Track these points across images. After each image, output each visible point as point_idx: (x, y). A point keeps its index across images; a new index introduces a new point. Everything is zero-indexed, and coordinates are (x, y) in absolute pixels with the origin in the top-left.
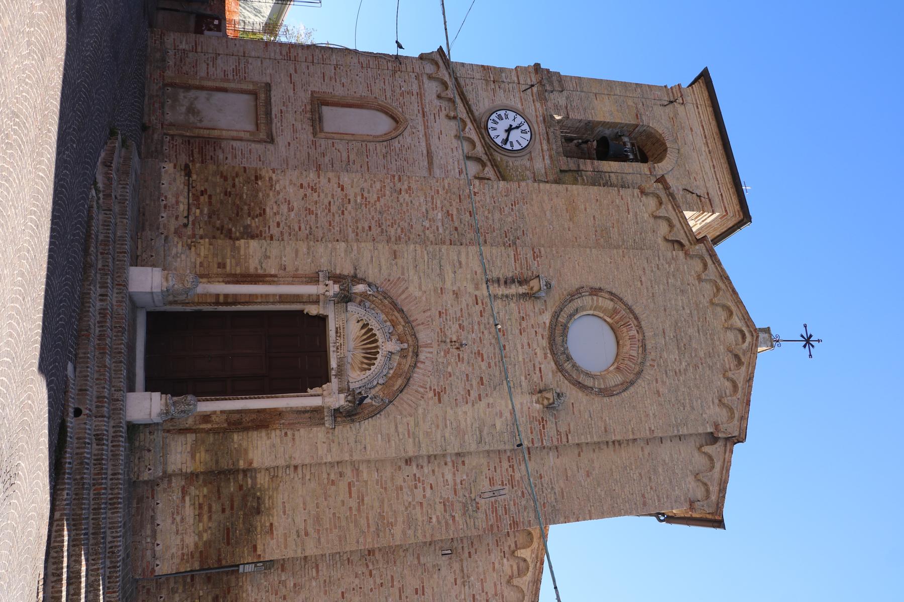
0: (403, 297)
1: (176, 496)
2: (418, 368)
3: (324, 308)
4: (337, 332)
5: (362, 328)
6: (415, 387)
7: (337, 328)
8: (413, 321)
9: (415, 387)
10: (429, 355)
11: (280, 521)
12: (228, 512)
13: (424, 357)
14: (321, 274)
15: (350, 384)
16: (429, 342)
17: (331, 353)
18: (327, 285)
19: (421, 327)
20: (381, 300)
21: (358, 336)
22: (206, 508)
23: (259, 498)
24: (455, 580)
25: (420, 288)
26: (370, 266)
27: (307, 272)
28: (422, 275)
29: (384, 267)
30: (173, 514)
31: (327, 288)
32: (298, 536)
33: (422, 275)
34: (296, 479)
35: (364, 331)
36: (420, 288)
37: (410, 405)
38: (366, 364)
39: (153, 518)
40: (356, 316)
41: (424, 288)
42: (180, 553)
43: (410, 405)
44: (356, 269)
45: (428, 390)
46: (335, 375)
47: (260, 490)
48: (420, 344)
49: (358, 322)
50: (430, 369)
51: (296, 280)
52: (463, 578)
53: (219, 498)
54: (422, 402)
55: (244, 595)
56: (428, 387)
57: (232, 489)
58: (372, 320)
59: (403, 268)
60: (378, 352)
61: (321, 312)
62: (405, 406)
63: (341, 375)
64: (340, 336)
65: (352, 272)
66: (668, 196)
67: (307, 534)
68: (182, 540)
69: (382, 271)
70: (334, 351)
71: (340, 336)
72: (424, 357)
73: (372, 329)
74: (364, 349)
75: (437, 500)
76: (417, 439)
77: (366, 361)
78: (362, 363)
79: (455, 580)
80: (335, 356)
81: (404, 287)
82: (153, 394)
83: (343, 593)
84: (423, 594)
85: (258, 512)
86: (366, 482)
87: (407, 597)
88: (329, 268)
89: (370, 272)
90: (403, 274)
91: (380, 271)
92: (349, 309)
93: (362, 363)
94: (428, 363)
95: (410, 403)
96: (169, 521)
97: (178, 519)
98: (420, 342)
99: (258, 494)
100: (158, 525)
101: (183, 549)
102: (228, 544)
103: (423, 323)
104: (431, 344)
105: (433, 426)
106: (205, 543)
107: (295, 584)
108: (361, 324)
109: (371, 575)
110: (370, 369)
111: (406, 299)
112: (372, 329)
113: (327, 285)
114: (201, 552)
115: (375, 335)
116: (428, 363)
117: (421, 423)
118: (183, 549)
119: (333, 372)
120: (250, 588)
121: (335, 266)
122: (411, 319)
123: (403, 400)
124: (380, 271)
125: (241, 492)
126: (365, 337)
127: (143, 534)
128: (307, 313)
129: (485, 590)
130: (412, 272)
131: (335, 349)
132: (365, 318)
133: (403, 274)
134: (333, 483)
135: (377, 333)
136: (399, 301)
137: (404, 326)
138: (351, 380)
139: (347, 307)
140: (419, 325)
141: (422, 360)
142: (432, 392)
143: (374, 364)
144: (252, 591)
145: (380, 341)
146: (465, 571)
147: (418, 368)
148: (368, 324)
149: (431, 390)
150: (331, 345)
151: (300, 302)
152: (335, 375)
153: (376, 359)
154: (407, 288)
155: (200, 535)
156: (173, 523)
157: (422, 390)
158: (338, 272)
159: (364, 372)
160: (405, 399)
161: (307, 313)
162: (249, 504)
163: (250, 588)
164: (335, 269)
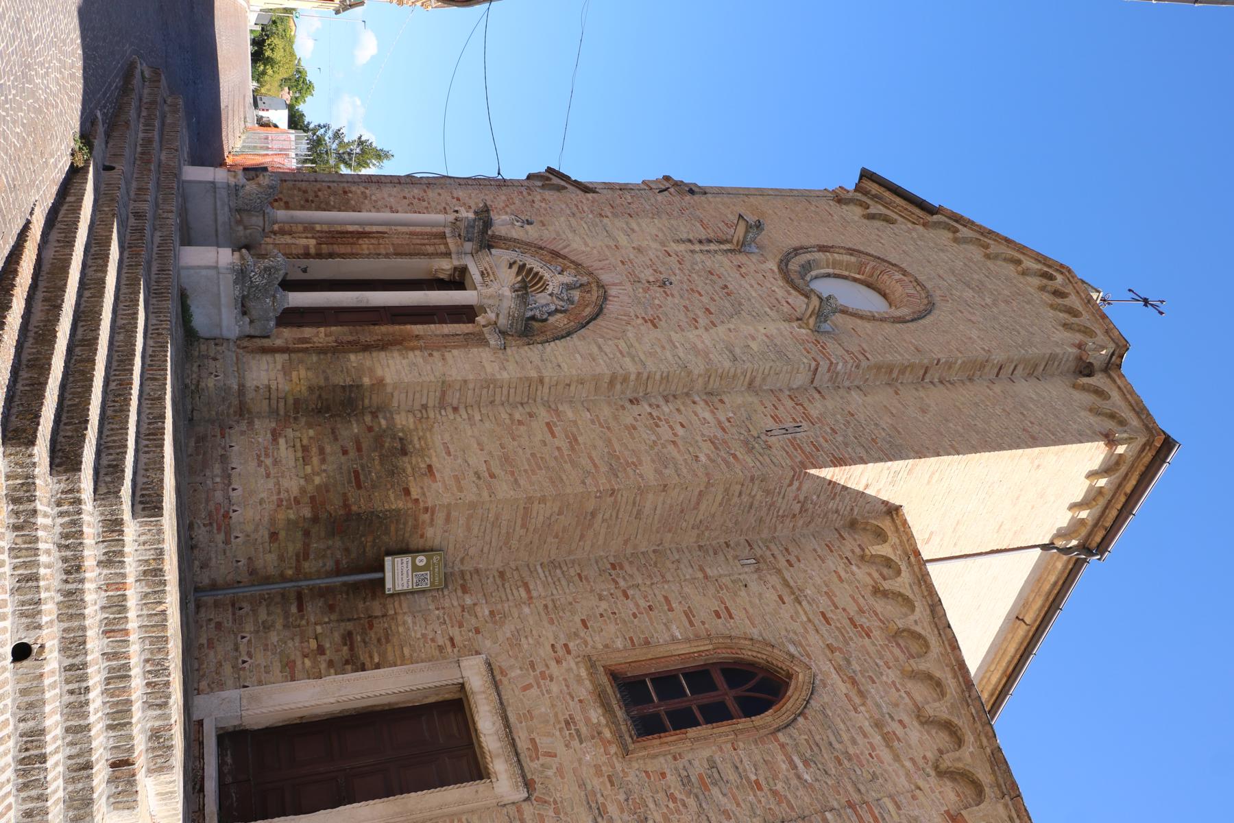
1: (263, 438)
3: (458, 259)
11: (445, 466)
12: (353, 454)
22: (314, 450)
23: (401, 439)
24: (780, 597)
30: (259, 456)
32: (479, 478)
34: (459, 419)
39: (224, 459)
42: (275, 498)
47: (402, 430)
49: (511, 266)
52: (793, 593)
53: (336, 439)
55: (401, 629)
57: (356, 431)
66: (872, 199)
67: (492, 476)
68: (278, 483)
73: (531, 269)
75: (699, 438)
76: (637, 359)
79: (780, 597)
82: (221, 250)
83: (583, 621)
84: (731, 617)
85: (404, 452)
86: (575, 422)
87: (703, 623)
96: (255, 463)
97: (269, 461)
99: (400, 434)
100: (233, 468)
101: (279, 493)
102: (359, 486)
106: (318, 488)
107: (492, 613)
108: (515, 269)
109: (627, 597)
114: (313, 498)
115: (537, 273)
118: (279, 493)
120: (409, 620)
125: (372, 434)
127: (208, 473)
129: (841, 605)
134: (520, 423)
144: (414, 623)
146: (792, 583)
155: (307, 478)
156: (259, 466)
162: (387, 445)
163: (409, 620)
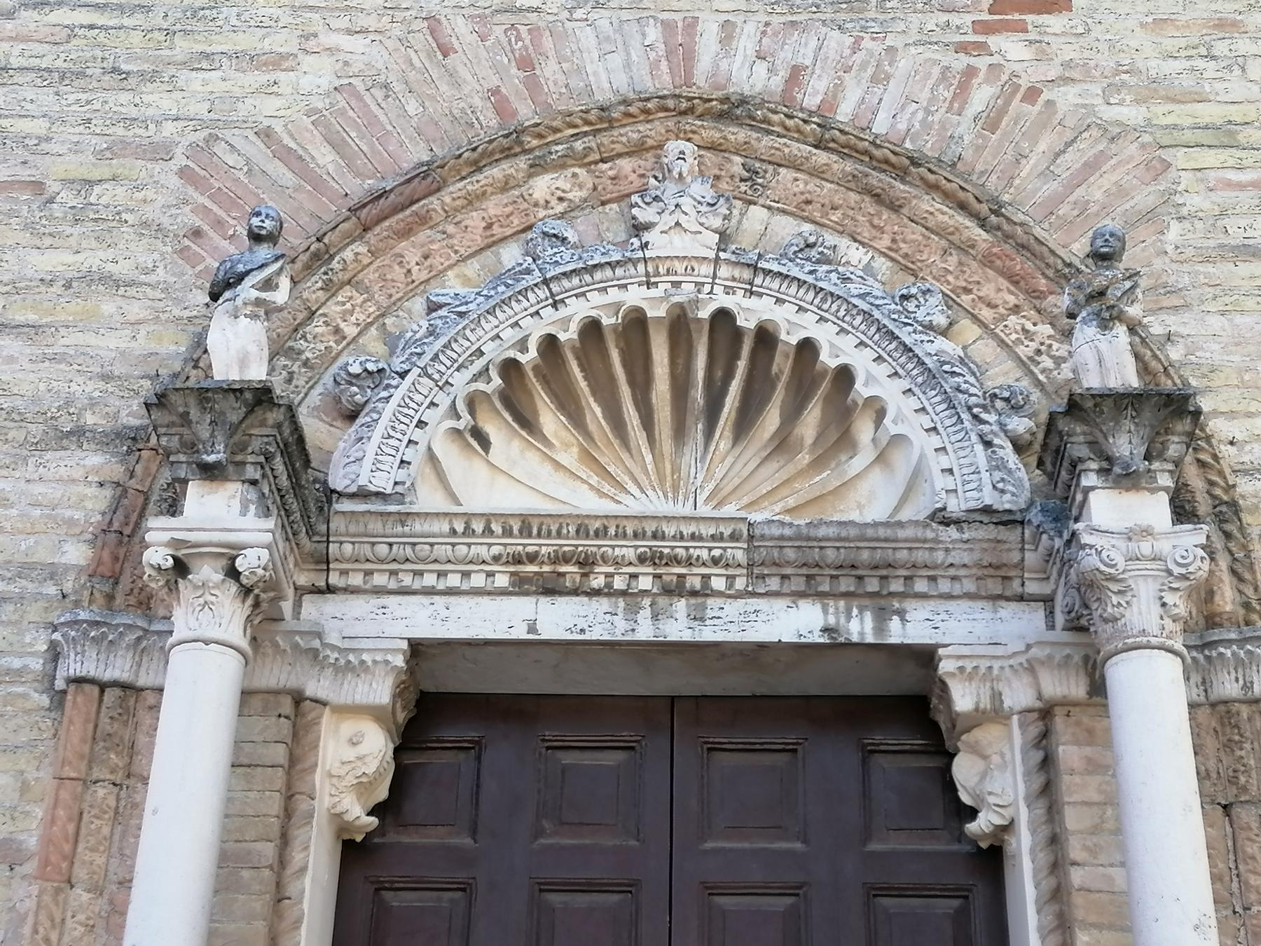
0: (325, 157)
2: (830, 102)
4: (551, 588)
5: (526, 422)
6: (965, 128)
7: (520, 586)
8: (501, 107)
9: (965, 128)
10: (746, 42)
13: (761, 68)
14: (73, 666)
15: (955, 506)
16: (653, 34)
17: (708, 634)
18: (181, 568)
19: (549, 71)
20: (331, 288)
21: (588, 458)
25: (278, 61)
26: (70, 339)
27: (42, 777)
28: (183, 47)
29: (94, 259)
31: (208, 572)
33: (183, 47)
35: (550, 420)
36: (278, 61)
37: (1092, 167)
38: (792, 414)
40: (438, 437)
41: (282, 42)
43: (1092, 167)
44: (79, 434)
45: (982, 63)
46: (882, 617)
48: (664, 82)
50: (837, 42)
51: (90, 859)
54: (1066, 98)
56: (960, 62)
58: (481, 336)
59: (115, 150)
60: (723, 317)
61: (380, 691)
62: (1096, 190)
63: (885, 568)
64: (586, 563)
65: (94, 459)
69: (122, 269)
70: (698, 617)
71: (586, 563)
72: (761, 68)
73: (550, 344)
74: (680, 432)
77: (771, 420)
78: (782, 444)
80: (733, 609)
81: (256, 150)
88: (34, 612)
89: (110, 343)
90: (161, 152)
91: (115, 283)
92: (382, 482)
93: (782, 444)
94: (800, 50)
95: (1072, 160)
98: (649, 85)
103: (526, 64)
104: (668, 27)
105: (1221, 48)
110: (845, 376)
111: (337, 145)
112: (550, 344)
113: (181, 568)
115: (592, 328)
116: (800, 50)
117: (1209, 113)
119: (860, 628)
121: (25, 569)
122: (490, 120)
123: (1060, 199)
124: (115, 283)
126: (595, 411)
128: (374, 811)
130: (158, 100)
131: (681, 606)
132: (460, 380)
133: (161, 152)
135: (578, 310)
136: (358, 187)
137: (537, 168)
138: (917, 510)
139: (363, 494)
140: (533, 85)
141: (777, 83)
142: (994, 41)
143: (807, 348)
145: (635, 296)
147: (830, 102)
148: (510, 368)
149: (982, 48)
150: (645, 631)
151: (285, 840)
152: (882, 617)
153: (765, 337)
154: (266, 135)
157: (981, 96)
158: (77, 554)
159: (864, 430)
160: (1051, 187)
161: (374, 811)
164: (53, 573)
